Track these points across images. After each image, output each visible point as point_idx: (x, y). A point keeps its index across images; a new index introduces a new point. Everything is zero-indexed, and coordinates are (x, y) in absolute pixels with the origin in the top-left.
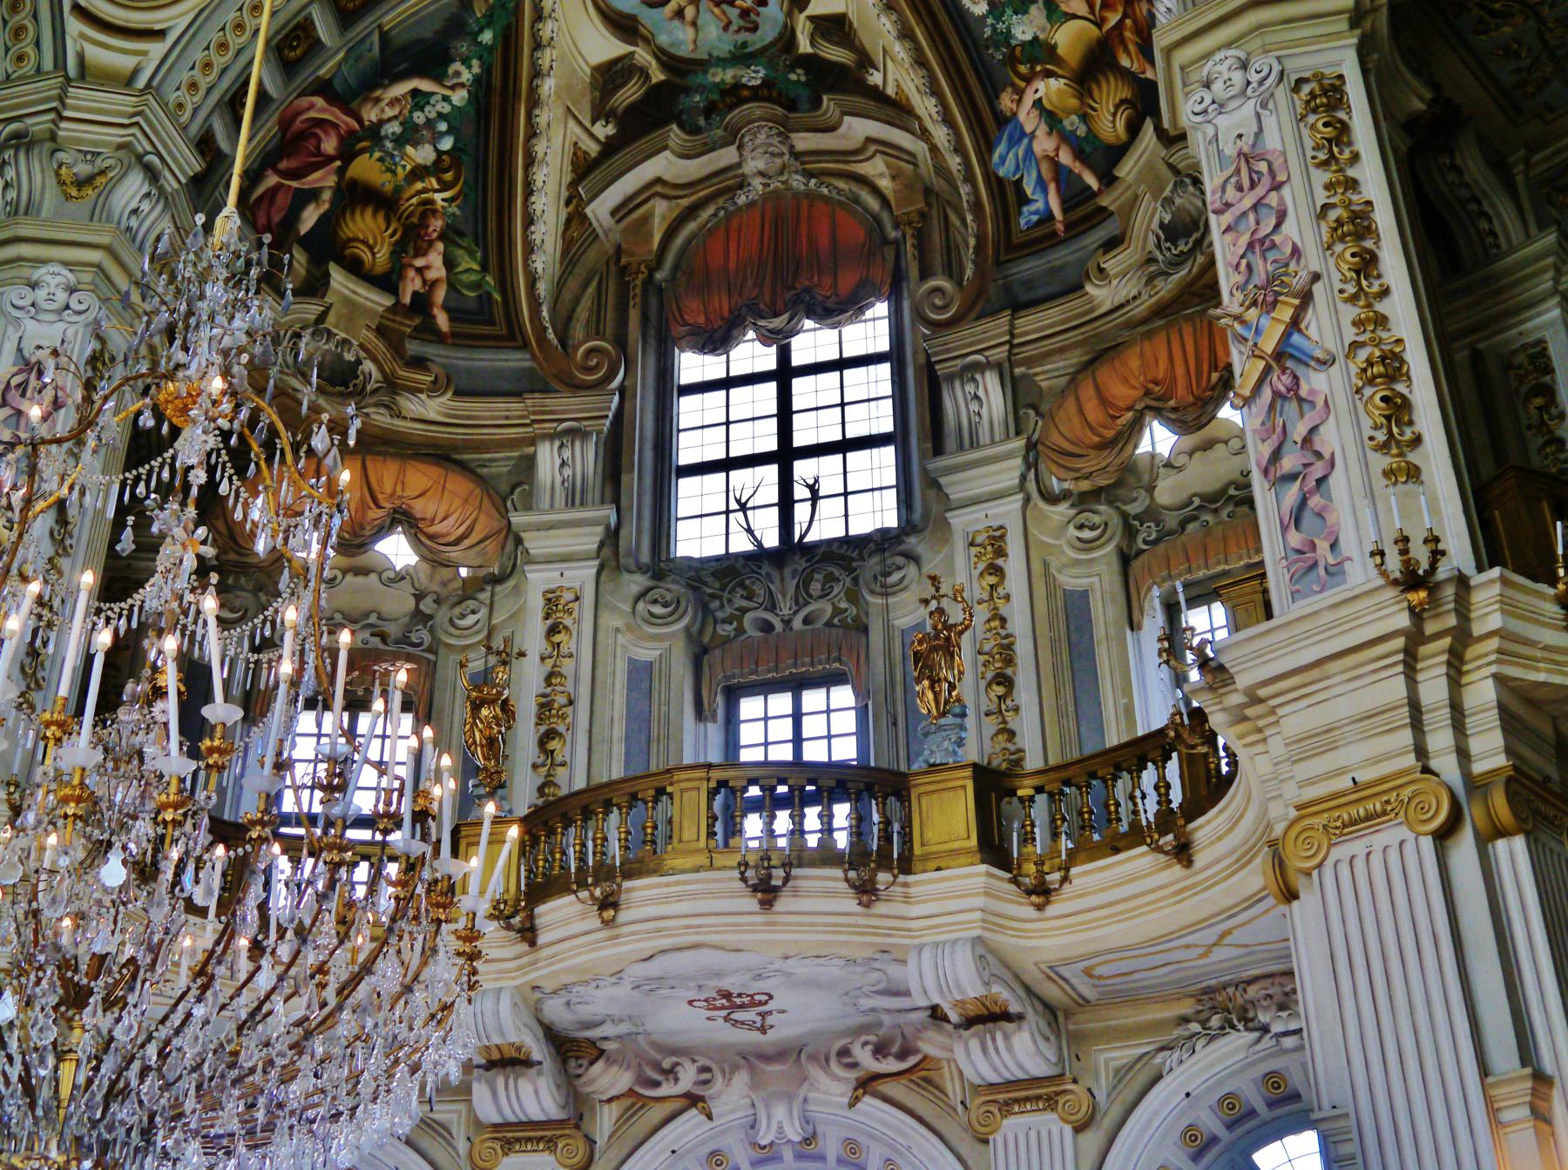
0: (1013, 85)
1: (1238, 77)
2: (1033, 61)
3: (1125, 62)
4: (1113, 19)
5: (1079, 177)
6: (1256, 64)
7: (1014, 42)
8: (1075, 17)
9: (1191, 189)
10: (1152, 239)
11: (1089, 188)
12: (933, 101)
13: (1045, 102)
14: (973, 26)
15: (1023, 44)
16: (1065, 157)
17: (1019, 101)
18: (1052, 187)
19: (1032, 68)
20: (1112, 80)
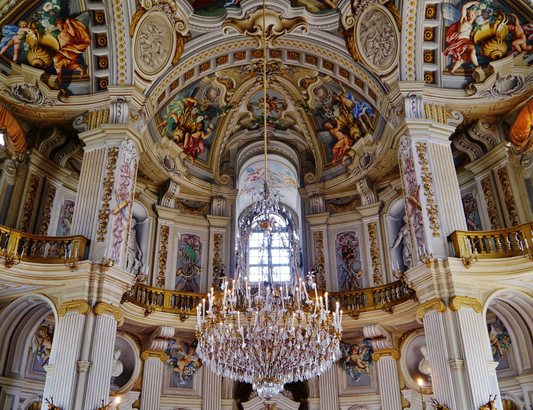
0: (28, 24)
1: (131, 147)
2: (37, 28)
3: (55, 60)
4: (66, 55)
5: (14, 54)
6: (134, 149)
7: (40, 21)
8: (58, 41)
9: (37, 93)
10: (14, 85)
11: (13, 58)
12: (14, 3)
13: (27, 35)
14: (40, 8)
15: (40, 24)
16: (16, 47)
17: (24, 27)
18: (7, 47)
19: (35, 28)
20: (46, 56)
